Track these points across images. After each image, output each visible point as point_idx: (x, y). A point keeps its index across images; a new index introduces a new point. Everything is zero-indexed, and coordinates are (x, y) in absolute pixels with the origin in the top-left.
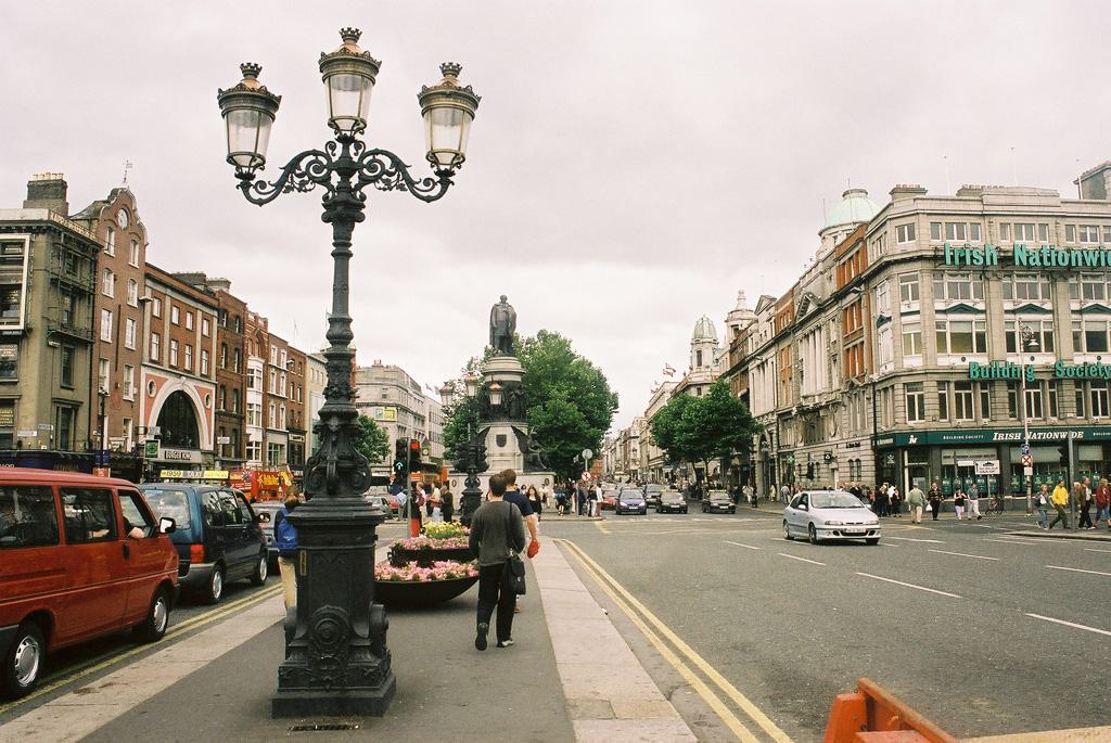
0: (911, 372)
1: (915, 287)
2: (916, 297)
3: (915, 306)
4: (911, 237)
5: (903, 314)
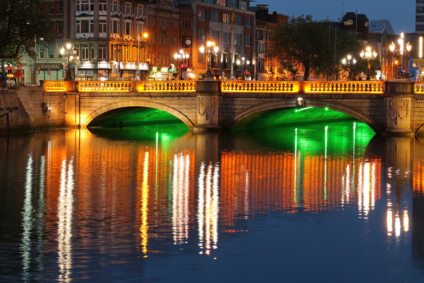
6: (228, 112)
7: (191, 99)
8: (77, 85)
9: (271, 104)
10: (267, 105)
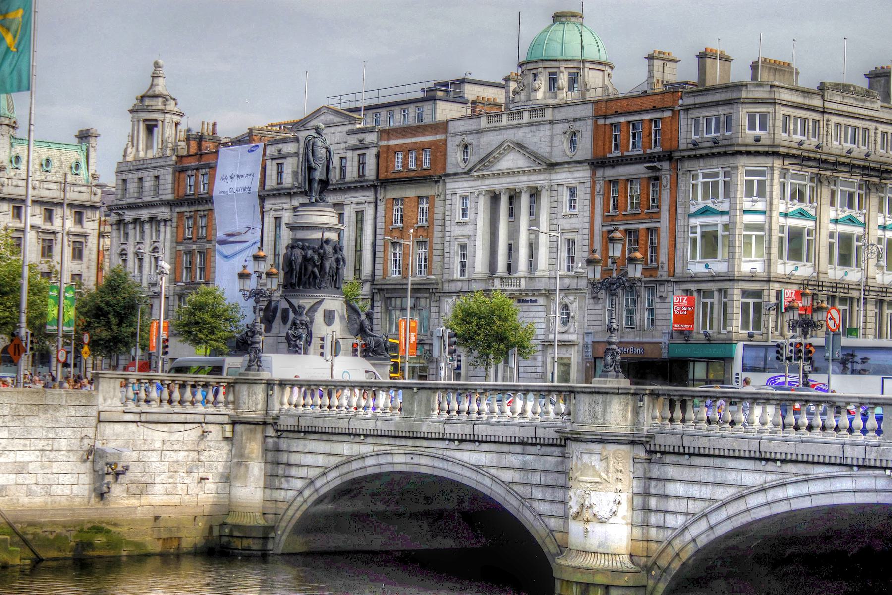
0: (752, 278)
1: (761, 184)
2: (761, 194)
3: (760, 205)
4: (763, 127)
5: (746, 212)
6: (666, 512)
7: (557, 453)
8: (271, 392)
9: (804, 489)
10: (791, 491)
